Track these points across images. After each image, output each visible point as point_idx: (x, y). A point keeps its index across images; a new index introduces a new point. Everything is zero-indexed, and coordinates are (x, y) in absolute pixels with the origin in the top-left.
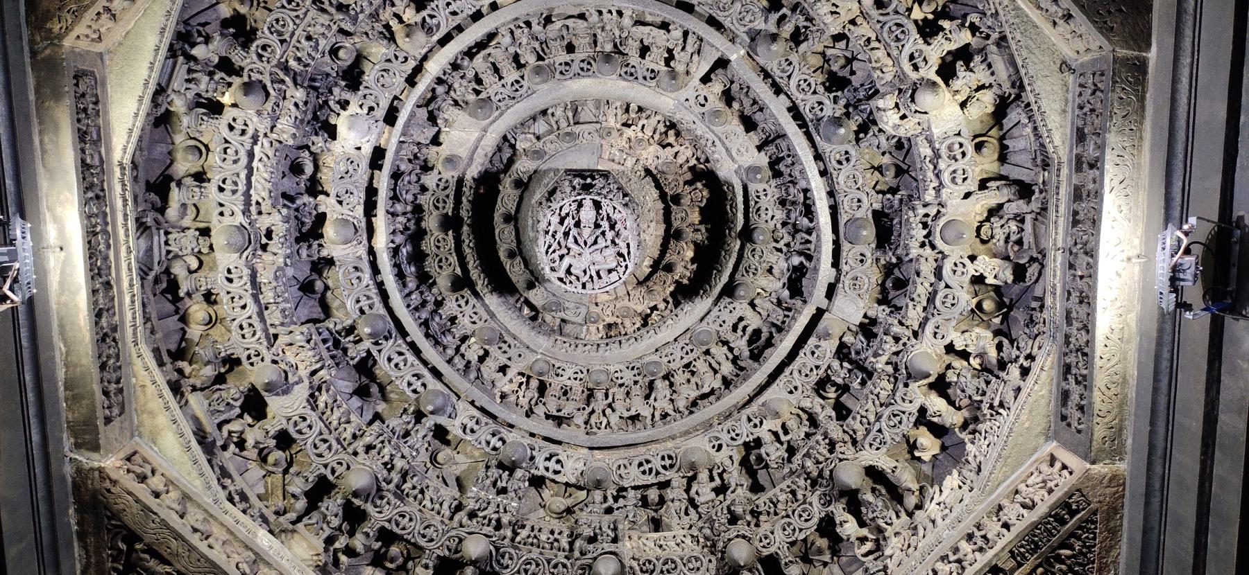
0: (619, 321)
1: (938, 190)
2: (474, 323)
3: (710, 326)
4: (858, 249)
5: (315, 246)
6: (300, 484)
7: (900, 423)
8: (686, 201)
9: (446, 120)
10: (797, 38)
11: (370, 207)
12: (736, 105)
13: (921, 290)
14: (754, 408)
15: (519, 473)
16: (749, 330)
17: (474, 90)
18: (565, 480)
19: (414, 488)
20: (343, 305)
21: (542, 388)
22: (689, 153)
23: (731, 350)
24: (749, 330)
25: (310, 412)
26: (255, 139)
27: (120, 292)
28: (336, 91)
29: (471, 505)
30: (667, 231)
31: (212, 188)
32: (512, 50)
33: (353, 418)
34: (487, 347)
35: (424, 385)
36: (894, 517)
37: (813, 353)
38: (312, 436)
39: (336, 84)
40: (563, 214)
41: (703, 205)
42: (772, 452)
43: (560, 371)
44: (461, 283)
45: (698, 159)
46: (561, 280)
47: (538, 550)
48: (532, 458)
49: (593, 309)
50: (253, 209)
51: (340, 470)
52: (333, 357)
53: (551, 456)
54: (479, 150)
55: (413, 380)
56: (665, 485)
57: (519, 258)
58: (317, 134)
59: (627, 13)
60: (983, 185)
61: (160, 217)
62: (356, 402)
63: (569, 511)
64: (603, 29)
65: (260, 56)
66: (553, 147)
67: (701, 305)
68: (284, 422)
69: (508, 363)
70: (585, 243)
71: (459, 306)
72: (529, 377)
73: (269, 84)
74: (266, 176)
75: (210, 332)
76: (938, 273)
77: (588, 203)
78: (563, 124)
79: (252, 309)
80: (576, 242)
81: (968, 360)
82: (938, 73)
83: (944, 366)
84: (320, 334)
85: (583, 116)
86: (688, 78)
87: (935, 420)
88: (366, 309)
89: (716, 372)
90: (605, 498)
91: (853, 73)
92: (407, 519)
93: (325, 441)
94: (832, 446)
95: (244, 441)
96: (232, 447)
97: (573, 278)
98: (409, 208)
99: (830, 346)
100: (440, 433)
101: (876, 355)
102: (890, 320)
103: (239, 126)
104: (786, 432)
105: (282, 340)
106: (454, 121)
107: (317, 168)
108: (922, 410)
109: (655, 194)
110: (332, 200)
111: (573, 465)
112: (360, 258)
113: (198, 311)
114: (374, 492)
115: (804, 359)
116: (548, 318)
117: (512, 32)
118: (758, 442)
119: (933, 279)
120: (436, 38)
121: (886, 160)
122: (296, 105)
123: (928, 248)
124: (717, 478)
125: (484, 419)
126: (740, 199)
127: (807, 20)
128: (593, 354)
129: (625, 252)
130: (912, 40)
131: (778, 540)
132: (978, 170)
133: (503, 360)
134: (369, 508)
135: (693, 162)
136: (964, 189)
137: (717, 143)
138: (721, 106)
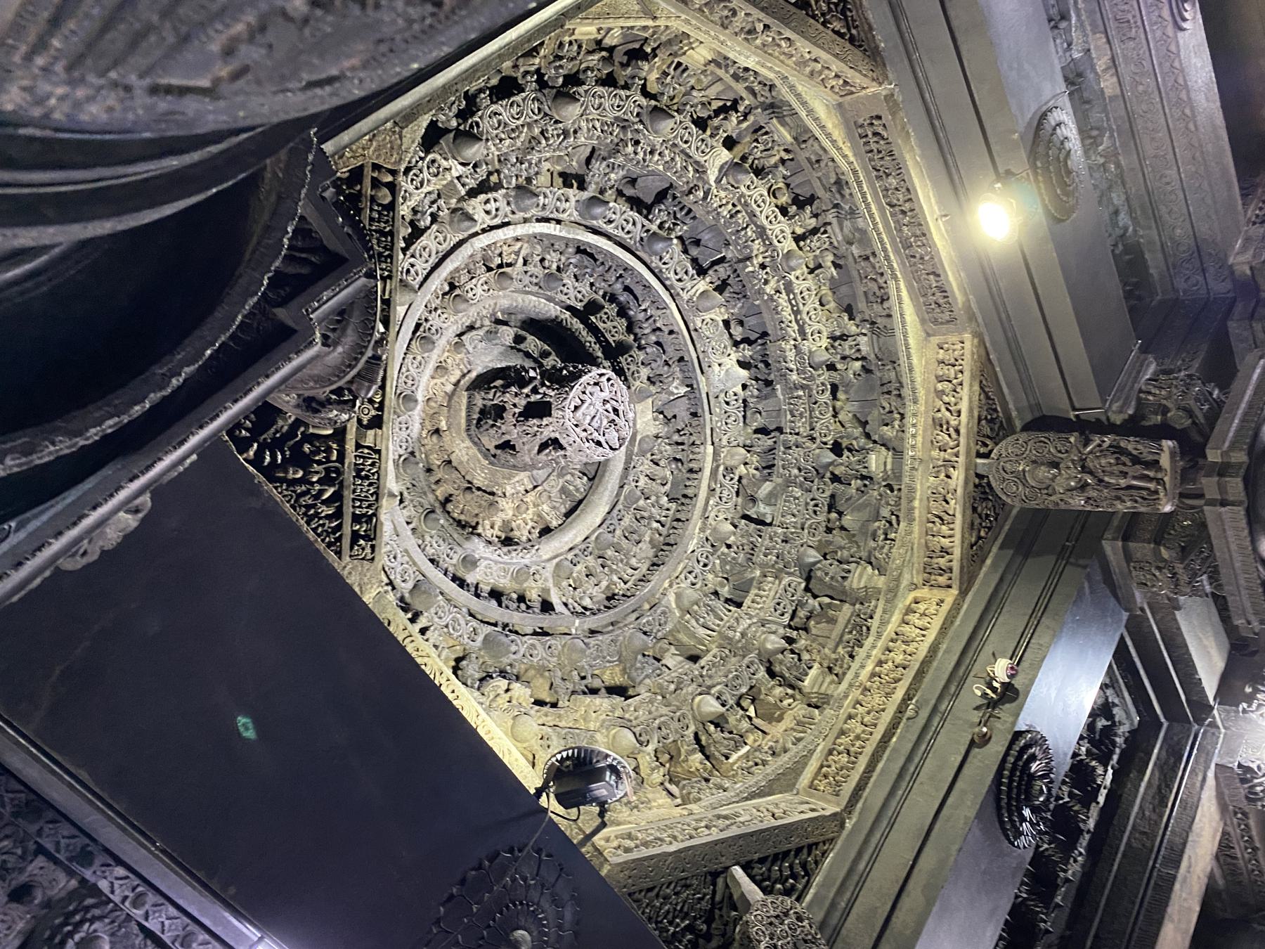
26: (802, 332)
28: (756, 392)
32: (653, 498)
48: (508, 204)
65: (823, 384)
109: (477, 483)
133: (530, 268)
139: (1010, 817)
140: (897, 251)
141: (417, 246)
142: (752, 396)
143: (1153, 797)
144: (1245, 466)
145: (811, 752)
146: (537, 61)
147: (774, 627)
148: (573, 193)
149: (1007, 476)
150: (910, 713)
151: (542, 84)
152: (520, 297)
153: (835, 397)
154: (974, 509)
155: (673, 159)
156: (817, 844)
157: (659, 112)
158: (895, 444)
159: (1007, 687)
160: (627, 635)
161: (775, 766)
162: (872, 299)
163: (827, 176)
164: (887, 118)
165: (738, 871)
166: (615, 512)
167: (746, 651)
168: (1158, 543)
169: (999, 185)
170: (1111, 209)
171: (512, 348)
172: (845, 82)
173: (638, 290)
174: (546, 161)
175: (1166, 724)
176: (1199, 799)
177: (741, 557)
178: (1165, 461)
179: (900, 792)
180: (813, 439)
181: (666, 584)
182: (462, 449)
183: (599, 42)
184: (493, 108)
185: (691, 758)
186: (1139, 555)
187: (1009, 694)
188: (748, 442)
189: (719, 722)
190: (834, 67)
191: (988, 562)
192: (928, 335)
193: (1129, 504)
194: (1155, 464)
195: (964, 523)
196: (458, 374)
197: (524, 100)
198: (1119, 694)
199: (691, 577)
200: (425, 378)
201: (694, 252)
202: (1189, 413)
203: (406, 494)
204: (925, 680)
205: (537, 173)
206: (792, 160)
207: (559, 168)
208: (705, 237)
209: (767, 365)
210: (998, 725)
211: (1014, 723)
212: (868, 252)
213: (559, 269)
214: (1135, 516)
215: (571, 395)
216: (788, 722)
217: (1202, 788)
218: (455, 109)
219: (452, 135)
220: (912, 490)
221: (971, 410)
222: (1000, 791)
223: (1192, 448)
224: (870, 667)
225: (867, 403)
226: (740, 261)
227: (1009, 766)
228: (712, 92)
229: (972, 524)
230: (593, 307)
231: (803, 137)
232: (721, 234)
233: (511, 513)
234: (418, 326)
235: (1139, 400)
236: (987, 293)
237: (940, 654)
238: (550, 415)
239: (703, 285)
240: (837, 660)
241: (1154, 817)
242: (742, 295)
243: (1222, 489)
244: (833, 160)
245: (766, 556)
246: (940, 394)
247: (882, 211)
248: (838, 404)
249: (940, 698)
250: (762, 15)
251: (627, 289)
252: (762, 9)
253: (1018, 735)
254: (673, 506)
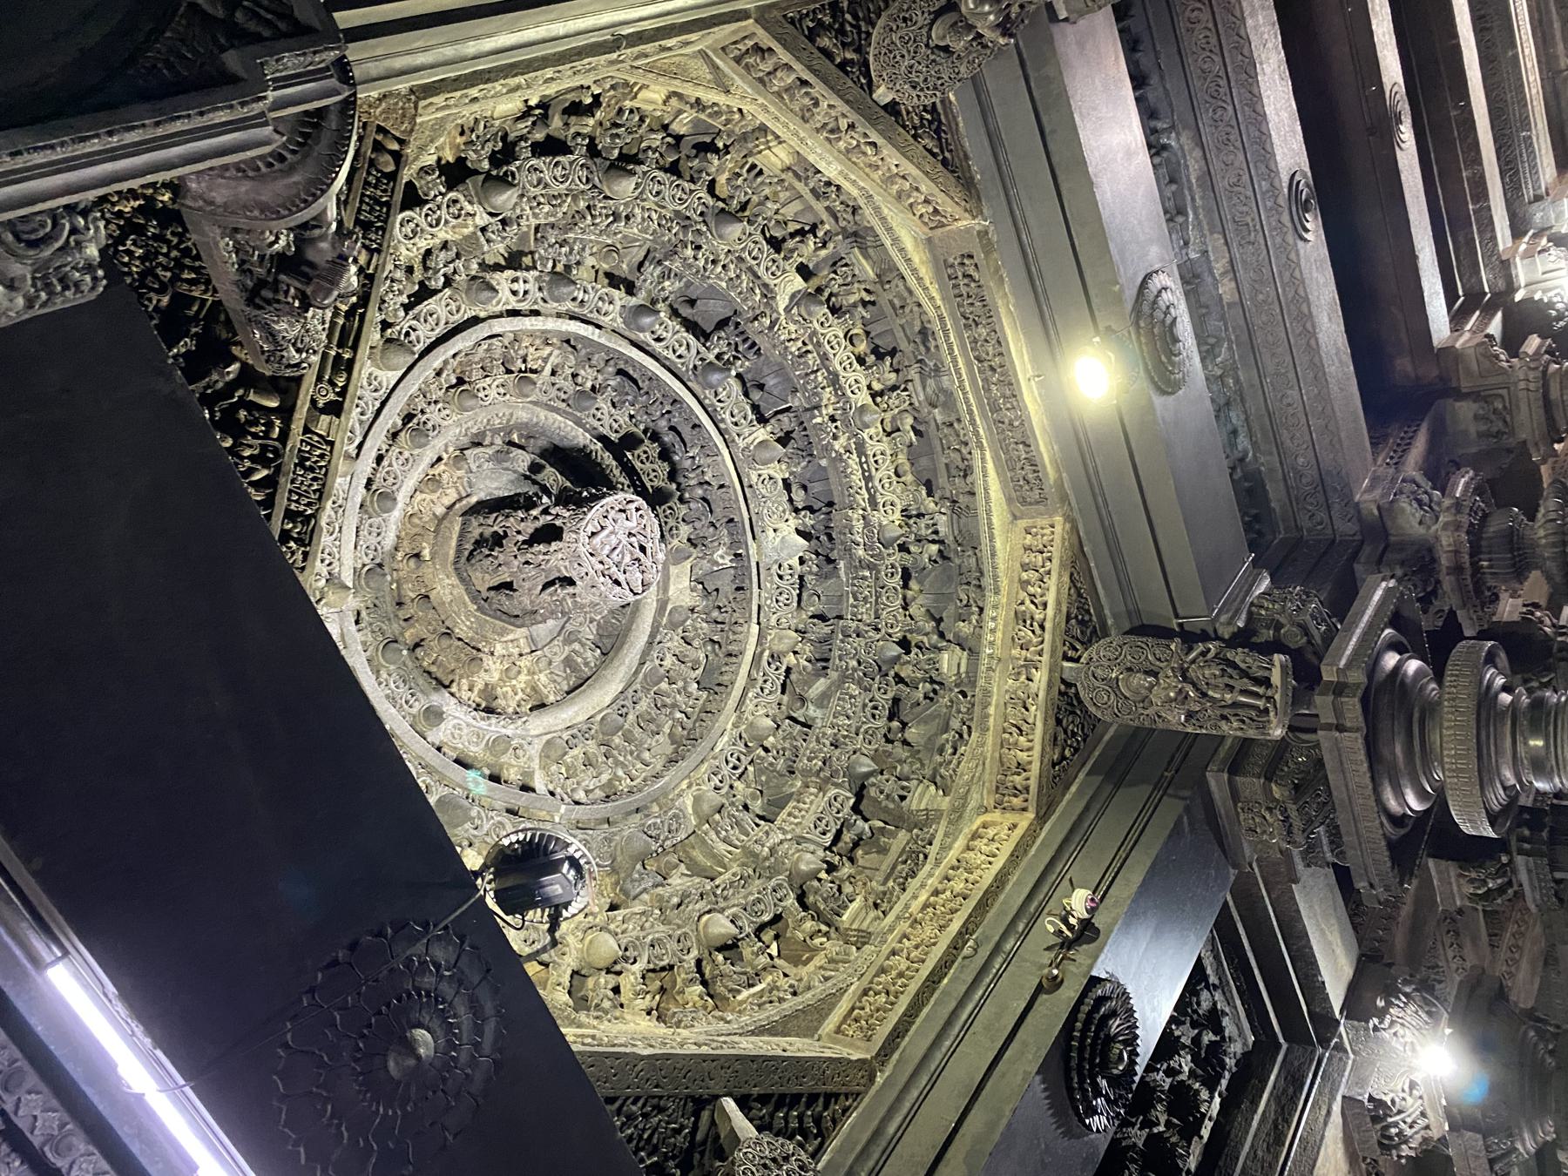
28: (815, 569)
31: (888, 452)
32: (680, 684)
48: (540, 289)
103: (888, 508)
133: (559, 380)
139: (1081, 1082)
140: (984, 416)
141: (423, 308)
142: (810, 573)
143: (1268, 1134)
144: (1363, 687)
145: (842, 991)
146: (591, 121)
147: (812, 847)
148: (618, 295)
149: (1097, 684)
150: (967, 951)
151: (593, 151)
152: (543, 414)
153: (906, 586)
154: (1059, 722)
155: (738, 277)
156: (837, 1096)
157: (727, 215)
158: (971, 643)
159: (1086, 924)
160: (626, 833)
161: (792, 1003)
162: (954, 472)
163: (911, 324)
164: (980, 256)
165: (729, 1104)
166: (631, 690)
167: (774, 871)
168: (1269, 779)
169: (1097, 339)
170: (1229, 427)
171: (526, 478)
172: (936, 211)
173: (686, 431)
174: (589, 247)
175: (1285, 1047)
176: (1323, 1137)
177: (781, 764)
178: (1276, 678)
179: (948, 1043)
180: (877, 630)
181: (684, 785)
182: (446, 587)
183: (665, 127)
184: (534, 162)
185: (687, 990)
186: (1247, 793)
187: (1087, 932)
188: (801, 626)
189: (730, 948)
190: (923, 188)
191: (1073, 789)
192: (1015, 517)
193: (1235, 724)
194: (1266, 682)
195: (1045, 733)
196: (453, 496)
197: (571, 163)
198: (1229, 1001)
199: (716, 781)
200: (410, 483)
201: (756, 395)
202: (1305, 630)
203: (364, 614)
204: (989, 915)
205: (578, 263)
206: (873, 303)
207: (605, 266)
208: (770, 382)
209: (830, 538)
210: (1072, 968)
211: (1091, 967)
212: (952, 419)
213: (593, 388)
214: (1245, 746)
215: (589, 516)
216: (819, 960)
217: (1326, 1124)
218: (489, 147)
219: (481, 177)
220: (987, 693)
221: (1058, 603)
222: (1069, 1048)
223: (1306, 673)
224: (923, 898)
225: (943, 597)
226: (807, 410)
227: (1082, 1016)
228: (789, 211)
229: (1056, 739)
230: (630, 441)
231: (887, 273)
232: (789, 380)
233: (496, 676)
234: (409, 417)
235: (1250, 613)
236: (1076, 449)
237: (1008, 887)
238: (560, 539)
239: (762, 433)
240: (884, 893)
241: (1269, 1158)
242: (807, 452)
243: (1338, 712)
244: (919, 305)
245: (810, 759)
246: (1024, 584)
247: (969, 365)
248: (910, 594)
249: (1004, 937)
250: (846, 109)
251: (672, 428)
252: (847, 102)
253: (1094, 981)
254: (704, 694)
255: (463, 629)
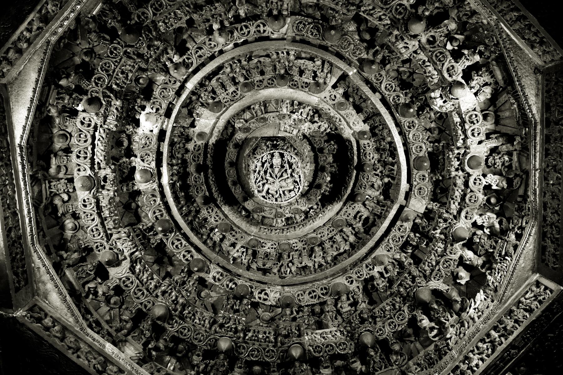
0: (293, 216)
1: (464, 140)
2: (217, 221)
3: (342, 217)
4: (421, 173)
5: (130, 185)
6: (128, 315)
7: (450, 265)
8: (326, 151)
9: (197, 114)
10: (384, 63)
11: (159, 164)
12: (351, 100)
13: (458, 194)
14: (369, 260)
15: (245, 301)
16: (363, 217)
17: (212, 97)
18: (270, 303)
19: (189, 313)
20: (147, 215)
21: (255, 254)
22: (326, 126)
23: (353, 229)
24: (363, 217)
25: (131, 275)
27: (23, 217)
28: (139, 101)
29: (221, 321)
30: (316, 167)
31: (73, 156)
32: (231, 75)
33: (155, 277)
34: (224, 233)
35: (192, 256)
36: (449, 316)
37: (399, 229)
38: (133, 288)
39: (139, 97)
40: (263, 161)
41: (335, 153)
42: (381, 284)
43: (264, 244)
44: (209, 201)
45: (331, 129)
46: (263, 197)
47: (258, 343)
48: (252, 293)
49: (279, 210)
50: (96, 166)
51: (149, 306)
52: (142, 244)
53: (262, 291)
54: (216, 129)
55: (186, 254)
56: (323, 303)
57: (238, 185)
58: (129, 125)
59: (292, 53)
60: (488, 136)
61: (46, 173)
62: (156, 267)
63: (273, 319)
64: (279, 62)
65: (97, 84)
66: (254, 125)
67: (337, 206)
68: (118, 281)
69: (236, 242)
70: (276, 176)
71: (209, 212)
72: (247, 249)
73: (102, 99)
74: (102, 148)
75: (77, 234)
76: (466, 184)
77: (277, 154)
78: (259, 113)
79: (97, 220)
80: (271, 176)
81: (483, 230)
82: (462, 77)
83: (471, 234)
84: (135, 232)
85: (269, 109)
86: (325, 86)
87: (468, 262)
88: (159, 217)
89: (346, 241)
90: (292, 313)
91: (414, 80)
92: (186, 331)
93: (140, 290)
94: (413, 279)
95: (98, 292)
96: (91, 296)
97: (270, 195)
98: (180, 161)
99: (408, 225)
100: (202, 282)
101: (435, 229)
102: (441, 211)
103: (86, 122)
104: (387, 273)
105: (115, 236)
106: (202, 114)
107: (130, 143)
108: (461, 257)
109: (309, 148)
110: (138, 159)
111: (274, 295)
112: (154, 190)
113: (69, 223)
114: (168, 316)
115: (395, 232)
116: (256, 216)
117: (231, 66)
118: (372, 278)
119: (463, 188)
120: (191, 70)
121: (433, 125)
122: (117, 109)
123: (460, 171)
124: (351, 298)
125: (225, 273)
126: (355, 148)
127: (389, 52)
128: (281, 234)
129: (298, 180)
130: (448, 60)
131: (387, 331)
132: (484, 129)
133: (233, 240)
134: (166, 325)
135: (329, 130)
136: (478, 139)
137: (342, 119)
138: (343, 100)
255: (306, 149)
